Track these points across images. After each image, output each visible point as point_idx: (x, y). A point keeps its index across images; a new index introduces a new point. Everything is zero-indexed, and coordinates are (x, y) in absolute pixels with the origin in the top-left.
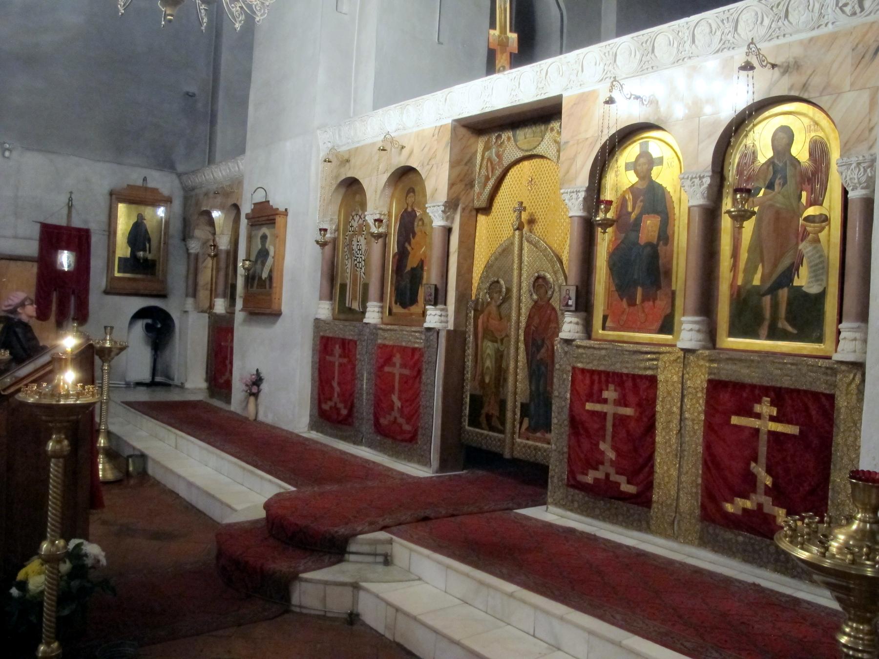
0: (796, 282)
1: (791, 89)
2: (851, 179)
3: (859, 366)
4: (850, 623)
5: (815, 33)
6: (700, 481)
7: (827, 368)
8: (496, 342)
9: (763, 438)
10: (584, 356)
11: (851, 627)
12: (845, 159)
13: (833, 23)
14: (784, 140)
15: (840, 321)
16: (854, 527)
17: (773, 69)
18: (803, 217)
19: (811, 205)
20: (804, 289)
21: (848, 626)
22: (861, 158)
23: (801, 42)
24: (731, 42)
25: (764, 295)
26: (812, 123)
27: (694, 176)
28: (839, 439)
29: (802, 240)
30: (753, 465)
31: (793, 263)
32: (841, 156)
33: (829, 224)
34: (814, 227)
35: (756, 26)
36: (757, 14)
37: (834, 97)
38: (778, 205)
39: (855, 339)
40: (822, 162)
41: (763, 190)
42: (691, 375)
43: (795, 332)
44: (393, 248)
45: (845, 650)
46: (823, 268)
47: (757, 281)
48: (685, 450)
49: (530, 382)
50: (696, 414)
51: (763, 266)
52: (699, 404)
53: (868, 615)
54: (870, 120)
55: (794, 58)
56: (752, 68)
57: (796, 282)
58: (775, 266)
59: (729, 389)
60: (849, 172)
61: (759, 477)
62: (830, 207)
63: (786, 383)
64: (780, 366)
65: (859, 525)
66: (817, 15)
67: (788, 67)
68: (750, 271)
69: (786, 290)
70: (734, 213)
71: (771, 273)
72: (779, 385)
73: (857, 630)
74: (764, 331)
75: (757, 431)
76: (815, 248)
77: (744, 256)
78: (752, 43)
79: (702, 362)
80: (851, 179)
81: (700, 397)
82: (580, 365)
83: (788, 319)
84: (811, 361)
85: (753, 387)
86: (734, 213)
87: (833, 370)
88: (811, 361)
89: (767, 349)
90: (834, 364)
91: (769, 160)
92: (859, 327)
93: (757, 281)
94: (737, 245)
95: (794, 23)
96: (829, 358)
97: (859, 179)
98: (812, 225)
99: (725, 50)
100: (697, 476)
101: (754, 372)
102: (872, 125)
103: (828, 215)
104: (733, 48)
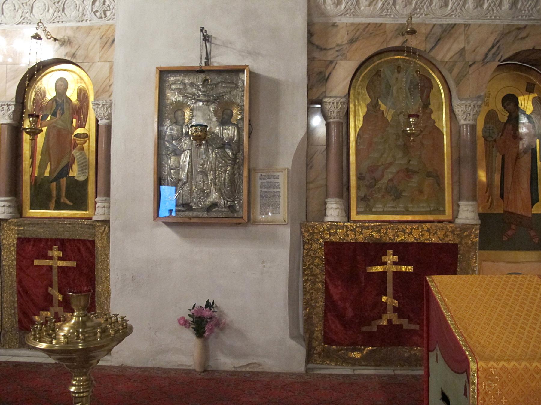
0: (71, 174)
1: (66, 55)
2: (99, 113)
3: (107, 222)
4: (75, 378)
5: (80, 24)
6: (16, 305)
7: (89, 225)
9: (55, 272)
11: (76, 380)
12: (96, 102)
13: (90, 20)
14: (63, 86)
15: (96, 197)
16: (73, 321)
17: (55, 41)
18: (74, 134)
19: (78, 128)
20: (76, 178)
21: (74, 380)
22: (105, 102)
23: (72, 28)
24: (28, 19)
25: (51, 182)
26: (79, 78)
27: (3, 104)
28: (99, 267)
29: (74, 149)
30: (50, 289)
31: (68, 163)
32: (94, 99)
33: (89, 139)
34: (80, 141)
35: (45, 13)
36: (45, 5)
37: (91, 63)
38: (59, 126)
39: (104, 207)
40: (84, 102)
41: (50, 116)
42: (5, 236)
43: (71, 204)
45: (74, 395)
46: (86, 165)
47: (47, 174)
48: (4, 286)
50: (10, 262)
51: (51, 164)
52: (12, 255)
53: (85, 370)
54: (110, 80)
55: (68, 37)
56: (40, 38)
57: (71, 174)
58: (58, 163)
59: (32, 243)
60: (99, 110)
61: (54, 296)
62: (89, 129)
63: (66, 236)
64: (63, 226)
65: (75, 319)
66: (81, 14)
67: (64, 41)
68: (42, 167)
69: (65, 179)
70: (28, 130)
71: (56, 168)
72: (62, 237)
73: (79, 381)
74: (53, 205)
75: (51, 267)
76: (81, 153)
77: (38, 157)
78: (40, 22)
79: (12, 227)
80: (99, 113)
81: (12, 250)
83: (66, 197)
84: (80, 222)
85: (47, 240)
86: (28, 130)
87: (92, 225)
88: (80, 222)
89: (55, 216)
90: (93, 222)
91: (54, 97)
92: (106, 200)
93: (47, 174)
94: (34, 151)
95: (68, 16)
96: (91, 219)
97: (104, 113)
98: (79, 139)
99: (24, 24)
100: (14, 302)
101: (47, 231)
102: (110, 83)
103: (88, 134)
104: (30, 23)
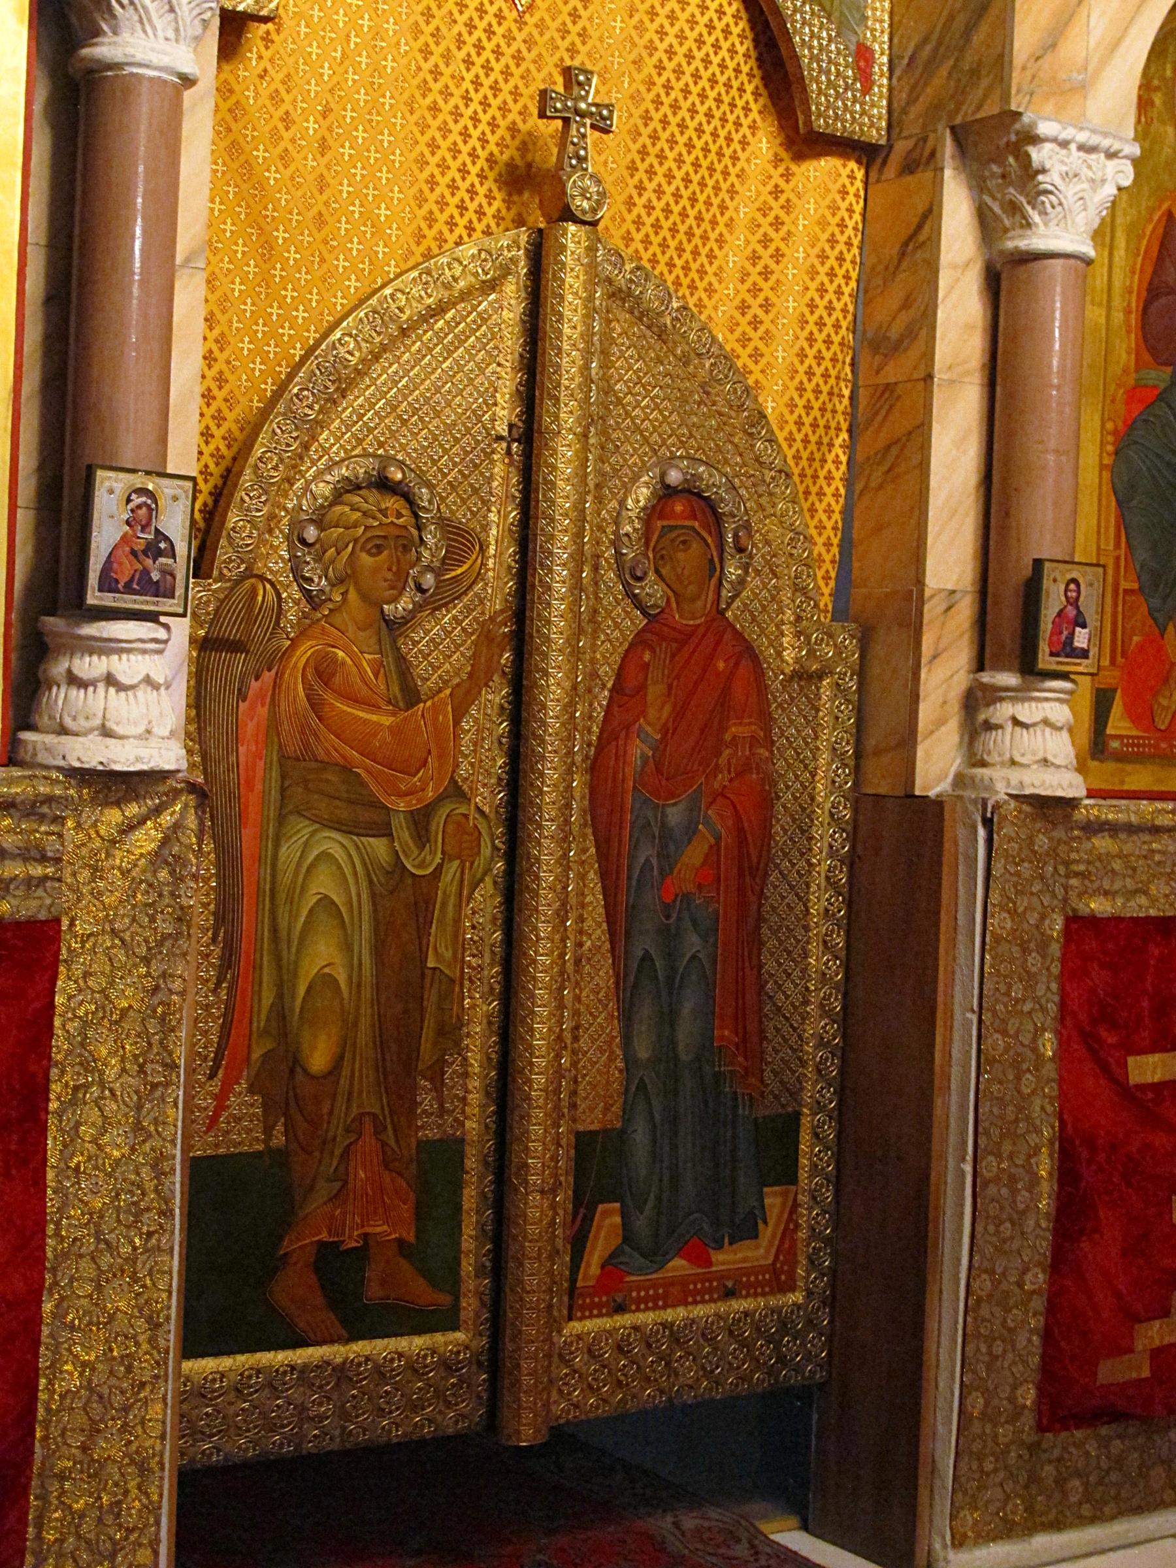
8: (384, 831)
10: (1117, 865)
44: (1088, 298)
49: (627, 1017)
82: (1098, 906)
